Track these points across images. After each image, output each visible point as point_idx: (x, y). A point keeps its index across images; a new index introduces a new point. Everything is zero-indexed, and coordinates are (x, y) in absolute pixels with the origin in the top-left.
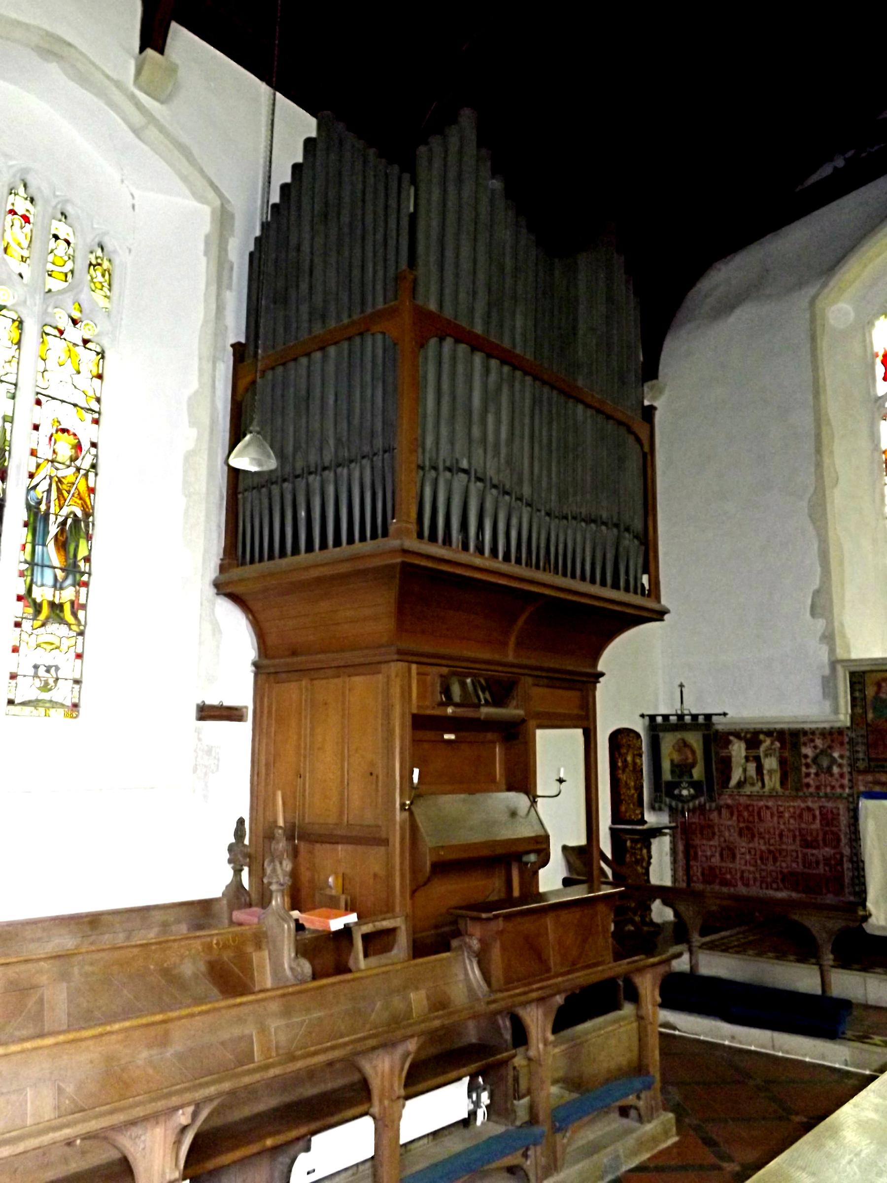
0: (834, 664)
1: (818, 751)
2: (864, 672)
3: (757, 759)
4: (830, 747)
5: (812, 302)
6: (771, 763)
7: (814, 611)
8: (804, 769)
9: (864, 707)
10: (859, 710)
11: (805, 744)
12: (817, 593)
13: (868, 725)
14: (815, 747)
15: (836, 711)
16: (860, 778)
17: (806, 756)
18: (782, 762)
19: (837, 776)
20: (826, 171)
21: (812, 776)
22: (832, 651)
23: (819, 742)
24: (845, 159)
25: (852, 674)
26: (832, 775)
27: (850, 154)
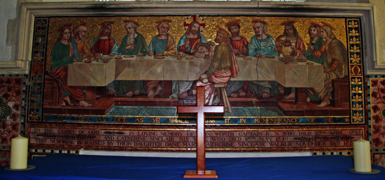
2: (49, 17)
9: (45, 55)
10: (39, 57)
13: (46, 73)
16: (33, 129)
25: (38, 19)
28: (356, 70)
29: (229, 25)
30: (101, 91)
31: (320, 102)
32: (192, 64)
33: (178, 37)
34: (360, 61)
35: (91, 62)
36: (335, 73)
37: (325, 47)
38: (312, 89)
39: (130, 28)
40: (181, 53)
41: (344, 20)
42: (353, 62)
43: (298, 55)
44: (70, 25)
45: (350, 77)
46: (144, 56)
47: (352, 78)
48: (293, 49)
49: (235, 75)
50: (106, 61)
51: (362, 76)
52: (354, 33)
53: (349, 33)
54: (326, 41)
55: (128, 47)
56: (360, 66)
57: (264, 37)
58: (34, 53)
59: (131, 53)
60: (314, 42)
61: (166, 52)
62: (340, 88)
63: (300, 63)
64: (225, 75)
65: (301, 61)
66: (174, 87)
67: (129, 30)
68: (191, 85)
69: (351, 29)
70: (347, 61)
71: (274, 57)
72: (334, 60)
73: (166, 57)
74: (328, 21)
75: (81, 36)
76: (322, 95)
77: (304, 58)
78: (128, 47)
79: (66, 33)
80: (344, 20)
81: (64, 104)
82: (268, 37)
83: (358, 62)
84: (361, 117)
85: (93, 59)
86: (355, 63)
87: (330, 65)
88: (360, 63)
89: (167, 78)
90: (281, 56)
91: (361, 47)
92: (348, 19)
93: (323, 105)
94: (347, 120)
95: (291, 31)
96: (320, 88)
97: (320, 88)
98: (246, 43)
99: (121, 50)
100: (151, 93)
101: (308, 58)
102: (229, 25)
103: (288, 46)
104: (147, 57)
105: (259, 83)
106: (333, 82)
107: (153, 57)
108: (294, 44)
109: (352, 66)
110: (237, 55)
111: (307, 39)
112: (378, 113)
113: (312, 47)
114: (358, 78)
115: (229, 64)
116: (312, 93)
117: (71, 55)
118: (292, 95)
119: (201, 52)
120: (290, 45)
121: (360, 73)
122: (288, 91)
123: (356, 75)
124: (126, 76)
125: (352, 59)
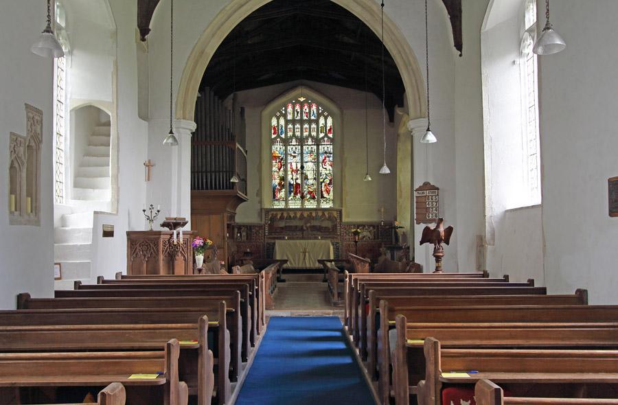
0: (261, 209)
3: (240, 233)
5: (261, 112)
6: (244, 234)
7: (257, 195)
15: (261, 220)
18: (247, 234)
23: (257, 228)
30: (282, 228)
33: (298, 215)
62: (335, 227)
99: (286, 219)
111: (327, 216)
124: (287, 224)
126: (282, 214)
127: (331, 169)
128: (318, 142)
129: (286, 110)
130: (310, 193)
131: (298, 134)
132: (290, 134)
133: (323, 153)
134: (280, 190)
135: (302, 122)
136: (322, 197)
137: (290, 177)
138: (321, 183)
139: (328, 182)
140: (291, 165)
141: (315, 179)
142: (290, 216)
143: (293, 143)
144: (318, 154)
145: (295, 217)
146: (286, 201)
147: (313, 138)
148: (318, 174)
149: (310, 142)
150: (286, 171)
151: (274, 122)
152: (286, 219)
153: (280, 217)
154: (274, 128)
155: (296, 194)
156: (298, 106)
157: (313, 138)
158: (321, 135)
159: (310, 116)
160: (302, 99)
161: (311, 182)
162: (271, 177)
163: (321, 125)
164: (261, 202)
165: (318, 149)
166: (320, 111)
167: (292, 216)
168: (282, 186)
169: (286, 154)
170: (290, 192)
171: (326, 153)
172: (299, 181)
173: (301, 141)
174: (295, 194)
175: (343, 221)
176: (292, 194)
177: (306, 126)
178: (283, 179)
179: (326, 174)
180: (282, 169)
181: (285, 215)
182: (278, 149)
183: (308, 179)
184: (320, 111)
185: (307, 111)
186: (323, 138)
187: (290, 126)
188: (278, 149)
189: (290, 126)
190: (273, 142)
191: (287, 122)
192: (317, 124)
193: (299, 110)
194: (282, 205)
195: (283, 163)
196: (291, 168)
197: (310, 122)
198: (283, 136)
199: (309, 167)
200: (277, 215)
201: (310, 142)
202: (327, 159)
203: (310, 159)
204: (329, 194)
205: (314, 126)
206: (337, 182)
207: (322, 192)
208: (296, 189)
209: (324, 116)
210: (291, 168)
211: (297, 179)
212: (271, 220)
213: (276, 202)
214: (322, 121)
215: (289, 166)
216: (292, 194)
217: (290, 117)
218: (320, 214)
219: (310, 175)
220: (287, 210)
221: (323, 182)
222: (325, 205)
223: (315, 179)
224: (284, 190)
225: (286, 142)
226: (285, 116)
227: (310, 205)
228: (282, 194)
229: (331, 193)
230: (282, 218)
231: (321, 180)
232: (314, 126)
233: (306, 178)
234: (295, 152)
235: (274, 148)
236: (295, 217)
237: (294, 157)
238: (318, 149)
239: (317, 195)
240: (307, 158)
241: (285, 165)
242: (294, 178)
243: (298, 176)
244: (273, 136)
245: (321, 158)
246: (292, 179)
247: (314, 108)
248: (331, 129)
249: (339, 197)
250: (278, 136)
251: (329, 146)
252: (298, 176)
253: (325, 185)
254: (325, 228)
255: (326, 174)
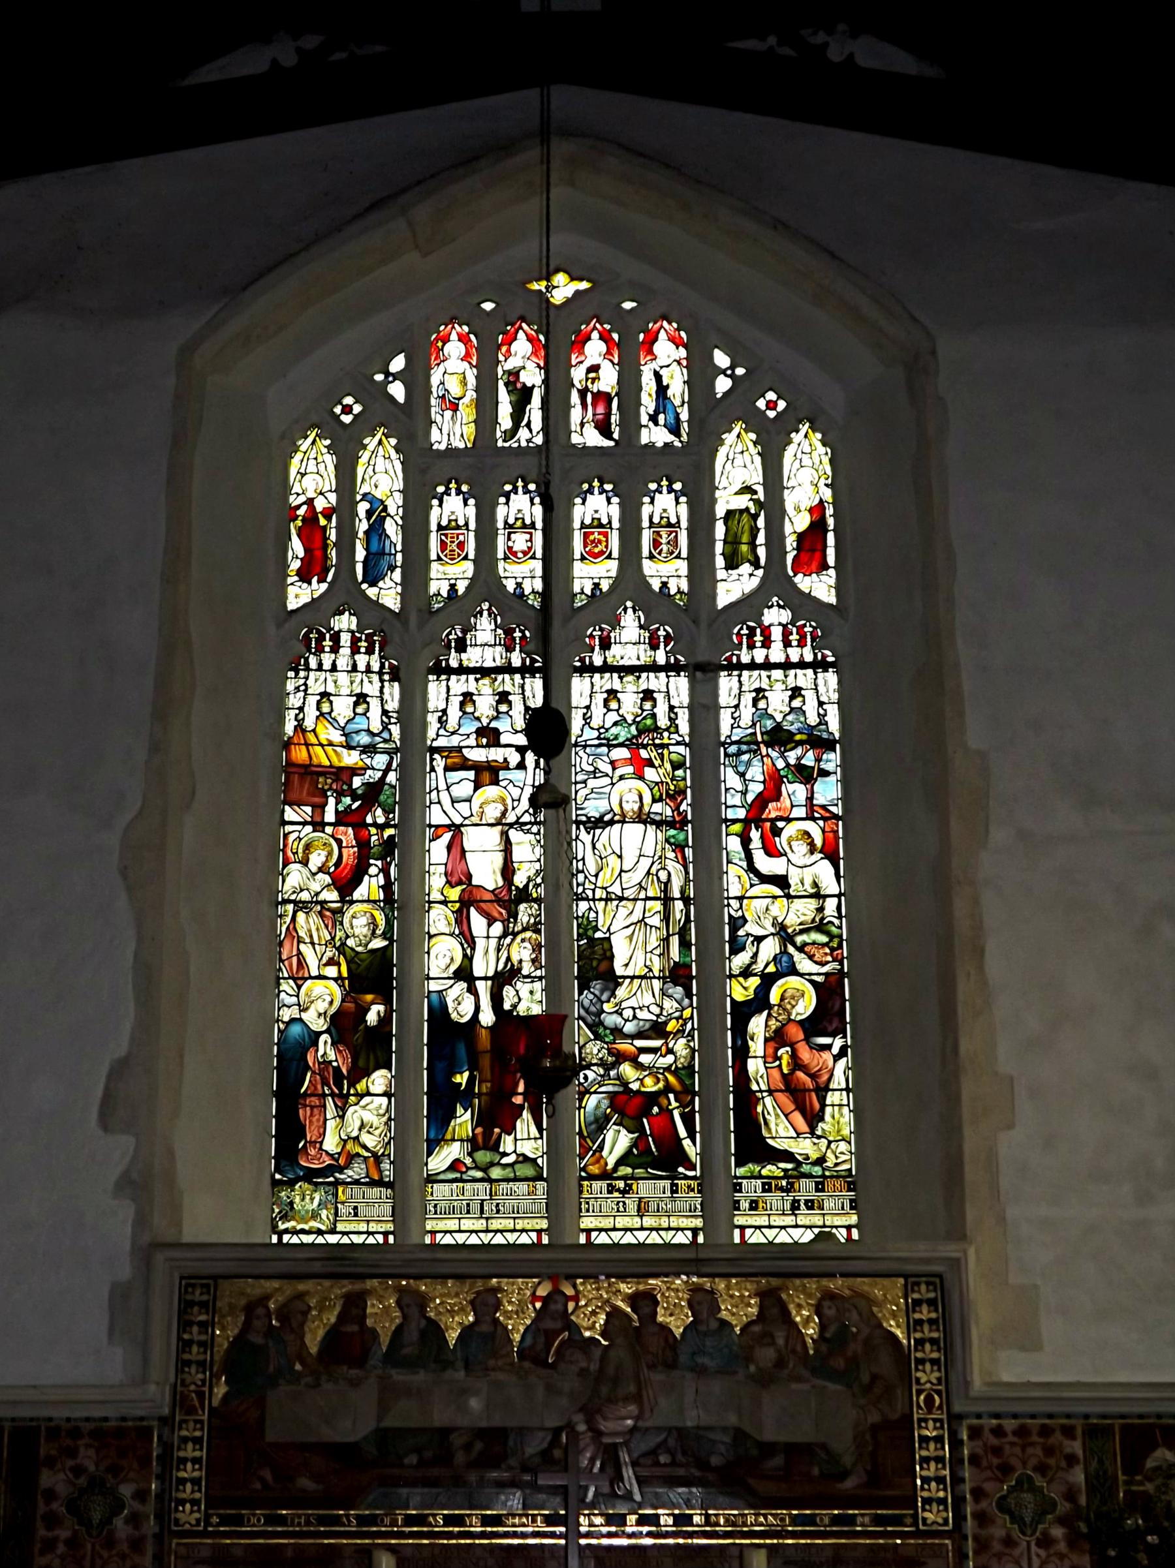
0: (147, 1252)
1: (82, 1481)
2: (216, 1278)
4: (115, 1470)
5: (187, 350)
7: (109, 1113)
8: (42, 1532)
11: (51, 1462)
12: (120, 1069)
14: (78, 1471)
17: (50, 1495)
19: (125, 1547)
20: (248, 63)
21: (61, 1549)
22: (141, 1221)
23: (88, 1458)
24: (299, 50)
25: (189, 1282)
26: (110, 1543)
27: (311, 42)
28: (929, 1401)
29: (633, 1299)
31: (844, 1475)
32: (550, 1389)
34: (939, 1379)
35: (319, 1385)
36: (880, 1410)
37: (855, 1347)
38: (824, 1446)
39: (408, 1306)
40: (527, 1364)
41: (902, 1281)
42: (922, 1381)
43: (791, 1365)
44: (266, 1298)
45: (915, 1416)
46: (444, 1369)
47: (920, 1420)
48: (779, 1351)
49: (647, 1414)
50: (355, 1383)
51: (945, 1417)
52: (925, 1313)
53: (914, 1311)
54: (859, 1331)
55: (405, 1351)
56: (939, 1393)
57: (714, 1325)
58: (182, 1365)
59: (411, 1364)
60: (828, 1335)
61: (491, 1363)
63: (794, 1386)
64: (623, 1412)
65: (799, 1379)
66: (511, 1443)
67: (406, 1310)
68: (549, 1438)
69: (917, 1303)
70: (906, 1378)
71: (735, 1373)
72: (874, 1378)
73: (492, 1373)
74: (863, 1284)
75: (294, 1325)
76: (848, 1460)
77: (805, 1373)
78: (405, 1351)
79: (258, 1318)
80: (902, 1281)
81: (258, 1486)
82: (725, 1324)
83: (935, 1381)
84: (944, 1514)
85: (324, 1378)
86: (928, 1386)
87: (868, 1389)
88: (939, 1383)
89: (497, 1421)
90: (752, 1368)
91: (942, 1345)
92: (911, 1280)
93: (849, 1484)
94: (909, 1521)
95: (775, 1311)
96: (843, 1445)
97: (843, 1445)
98: (671, 1340)
100: (460, 1458)
101: (815, 1372)
102: (633, 1299)
103: (769, 1345)
104: (449, 1374)
105: (701, 1433)
106: (874, 1428)
107: (462, 1373)
108: (781, 1342)
109: (919, 1392)
110: (652, 1367)
112: (984, 1504)
113: (824, 1348)
114: (935, 1421)
115: (632, 1388)
116: (823, 1455)
117: (271, 1368)
118: (778, 1461)
119: (572, 1362)
120: (773, 1343)
121: (940, 1407)
122: (769, 1449)
123: (930, 1412)
124: (405, 1414)
125: (919, 1374)
126: (354, 1305)
127: (830, 885)
128: (701, 641)
129: (417, 379)
130: (629, 1106)
131: (523, 574)
132: (449, 575)
133: (750, 744)
134: (344, 1086)
135: (554, 474)
136: (754, 1146)
137: (443, 953)
138: (743, 1012)
139: (805, 1007)
140: (456, 848)
141: (677, 975)
142: (435, 1331)
143: (472, 657)
144: (706, 746)
145: (485, 1335)
146: (404, 1187)
147: (654, 605)
148: (702, 934)
149: (629, 641)
150: (401, 904)
151: (311, 475)
152: (393, 1357)
153: (333, 1335)
154: (311, 528)
155: (496, 1119)
156: (522, 346)
157: (654, 605)
158: (734, 586)
159: (631, 425)
160: (563, 288)
161: (638, 1002)
162: (272, 962)
163: (727, 500)
164: (144, 1185)
165: (704, 708)
166: (723, 385)
167: (453, 1336)
168: (366, 1046)
169: (413, 752)
170: (443, 1104)
171: (779, 738)
172: (528, 999)
173: (552, 633)
174: (484, 1120)
175: (977, 1383)
176: (464, 1121)
177: (596, 506)
178: (371, 975)
179: (784, 934)
180: (370, 887)
181: (383, 1312)
182: (343, 707)
183: (612, 981)
184: (723, 385)
185: (608, 380)
186: (750, 605)
187: (454, 507)
188: (336, 702)
189: (454, 507)
190: (307, 637)
191: (426, 473)
192: (699, 494)
193: (532, 377)
194: (365, 1223)
195: (383, 825)
196: (459, 876)
197: (629, 470)
198: (388, 593)
199: (627, 858)
200: (294, 1315)
201: (629, 641)
202: (799, 791)
203: (629, 793)
204: (814, 1118)
205: (666, 505)
206: (900, 988)
207: (746, 1099)
208: (518, 1065)
209: (755, 422)
210: (459, 876)
211: (506, 976)
212: (243, 1362)
213: (307, 1199)
214: (736, 467)
215: (438, 851)
216: (464, 1121)
217: (451, 431)
218: (738, 1306)
219: (633, 950)
220: (411, 1263)
221: (760, 1002)
222: (772, 1225)
223: (677, 975)
224: (379, 1080)
225: (414, 644)
226: (409, 424)
227: (662, 1218)
228: (364, 1118)
229: (839, 1116)
230: (348, 1344)
231: (740, 991)
232: (666, 505)
233: (597, 966)
234: (489, 735)
235: (300, 698)
236: (485, 1335)
237: (487, 774)
238: (704, 708)
239: (700, 1124)
240: (607, 787)
241: (400, 850)
242: (483, 966)
243: (521, 952)
244: (298, 595)
245: (737, 787)
246: (464, 974)
247: (667, 355)
248: (818, 527)
249: (922, 1151)
250: (346, 596)
251: (804, 678)
252: (521, 952)
253: (777, 1038)
254: (796, 1452)
255: (784, 934)
